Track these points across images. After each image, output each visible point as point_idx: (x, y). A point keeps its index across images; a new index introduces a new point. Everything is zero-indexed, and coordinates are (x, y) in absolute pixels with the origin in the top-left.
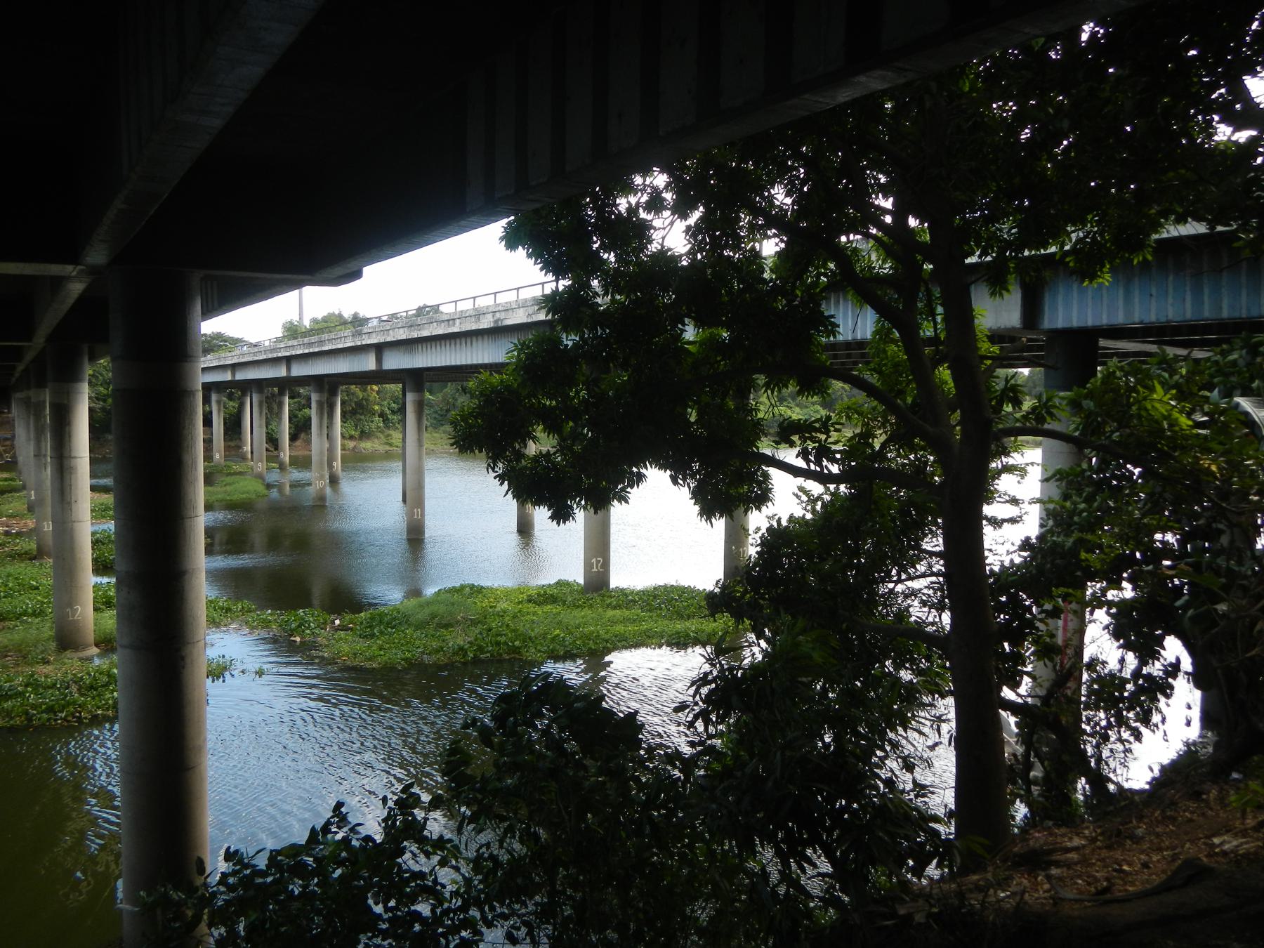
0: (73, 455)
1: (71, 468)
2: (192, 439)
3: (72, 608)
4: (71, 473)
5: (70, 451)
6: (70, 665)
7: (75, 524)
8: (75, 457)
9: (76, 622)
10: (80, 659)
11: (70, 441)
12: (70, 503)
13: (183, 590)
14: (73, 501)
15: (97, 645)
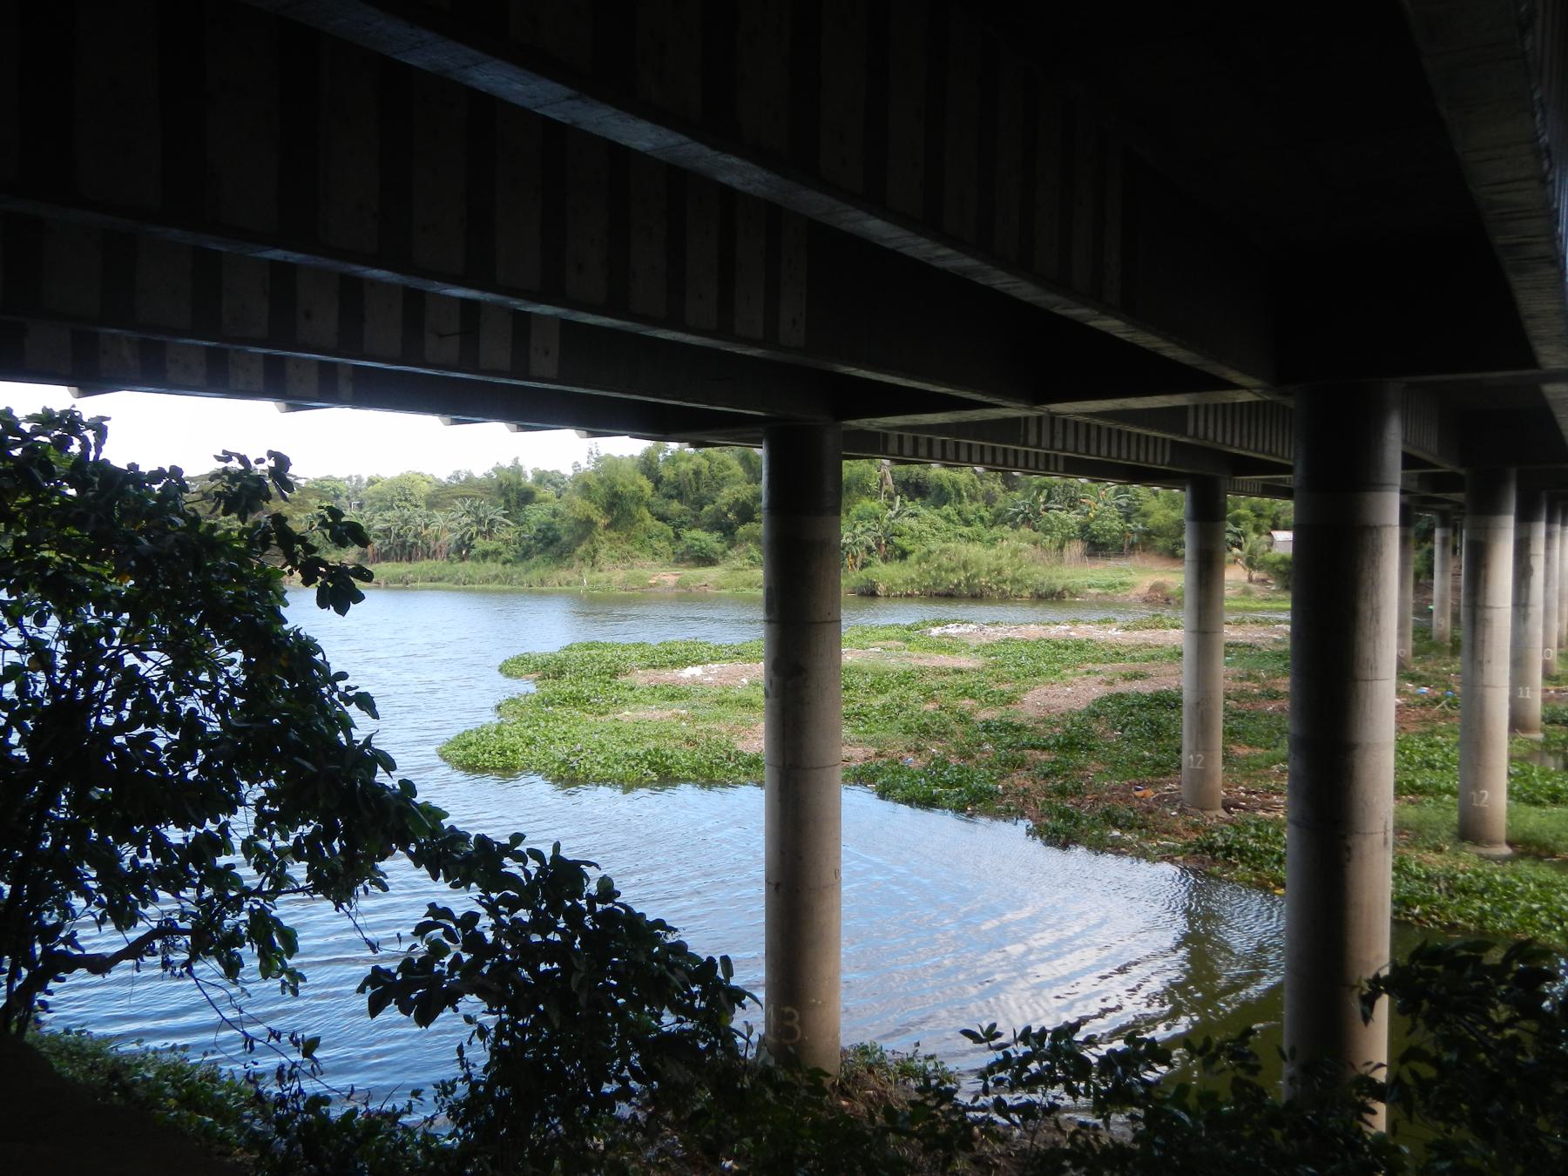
0: (1489, 603)
1: (1486, 619)
2: (1373, 584)
3: (1478, 792)
4: (1484, 626)
5: (1485, 598)
6: (1466, 862)
7: (1488, 690)
8: (1491, 608)
9: (1480, 810)
10: (1480, 856)
11: (1485, 588)
12: (1481, 663)
13: (1353, 767)
14: (1485, 660)
15: (1510, 844)
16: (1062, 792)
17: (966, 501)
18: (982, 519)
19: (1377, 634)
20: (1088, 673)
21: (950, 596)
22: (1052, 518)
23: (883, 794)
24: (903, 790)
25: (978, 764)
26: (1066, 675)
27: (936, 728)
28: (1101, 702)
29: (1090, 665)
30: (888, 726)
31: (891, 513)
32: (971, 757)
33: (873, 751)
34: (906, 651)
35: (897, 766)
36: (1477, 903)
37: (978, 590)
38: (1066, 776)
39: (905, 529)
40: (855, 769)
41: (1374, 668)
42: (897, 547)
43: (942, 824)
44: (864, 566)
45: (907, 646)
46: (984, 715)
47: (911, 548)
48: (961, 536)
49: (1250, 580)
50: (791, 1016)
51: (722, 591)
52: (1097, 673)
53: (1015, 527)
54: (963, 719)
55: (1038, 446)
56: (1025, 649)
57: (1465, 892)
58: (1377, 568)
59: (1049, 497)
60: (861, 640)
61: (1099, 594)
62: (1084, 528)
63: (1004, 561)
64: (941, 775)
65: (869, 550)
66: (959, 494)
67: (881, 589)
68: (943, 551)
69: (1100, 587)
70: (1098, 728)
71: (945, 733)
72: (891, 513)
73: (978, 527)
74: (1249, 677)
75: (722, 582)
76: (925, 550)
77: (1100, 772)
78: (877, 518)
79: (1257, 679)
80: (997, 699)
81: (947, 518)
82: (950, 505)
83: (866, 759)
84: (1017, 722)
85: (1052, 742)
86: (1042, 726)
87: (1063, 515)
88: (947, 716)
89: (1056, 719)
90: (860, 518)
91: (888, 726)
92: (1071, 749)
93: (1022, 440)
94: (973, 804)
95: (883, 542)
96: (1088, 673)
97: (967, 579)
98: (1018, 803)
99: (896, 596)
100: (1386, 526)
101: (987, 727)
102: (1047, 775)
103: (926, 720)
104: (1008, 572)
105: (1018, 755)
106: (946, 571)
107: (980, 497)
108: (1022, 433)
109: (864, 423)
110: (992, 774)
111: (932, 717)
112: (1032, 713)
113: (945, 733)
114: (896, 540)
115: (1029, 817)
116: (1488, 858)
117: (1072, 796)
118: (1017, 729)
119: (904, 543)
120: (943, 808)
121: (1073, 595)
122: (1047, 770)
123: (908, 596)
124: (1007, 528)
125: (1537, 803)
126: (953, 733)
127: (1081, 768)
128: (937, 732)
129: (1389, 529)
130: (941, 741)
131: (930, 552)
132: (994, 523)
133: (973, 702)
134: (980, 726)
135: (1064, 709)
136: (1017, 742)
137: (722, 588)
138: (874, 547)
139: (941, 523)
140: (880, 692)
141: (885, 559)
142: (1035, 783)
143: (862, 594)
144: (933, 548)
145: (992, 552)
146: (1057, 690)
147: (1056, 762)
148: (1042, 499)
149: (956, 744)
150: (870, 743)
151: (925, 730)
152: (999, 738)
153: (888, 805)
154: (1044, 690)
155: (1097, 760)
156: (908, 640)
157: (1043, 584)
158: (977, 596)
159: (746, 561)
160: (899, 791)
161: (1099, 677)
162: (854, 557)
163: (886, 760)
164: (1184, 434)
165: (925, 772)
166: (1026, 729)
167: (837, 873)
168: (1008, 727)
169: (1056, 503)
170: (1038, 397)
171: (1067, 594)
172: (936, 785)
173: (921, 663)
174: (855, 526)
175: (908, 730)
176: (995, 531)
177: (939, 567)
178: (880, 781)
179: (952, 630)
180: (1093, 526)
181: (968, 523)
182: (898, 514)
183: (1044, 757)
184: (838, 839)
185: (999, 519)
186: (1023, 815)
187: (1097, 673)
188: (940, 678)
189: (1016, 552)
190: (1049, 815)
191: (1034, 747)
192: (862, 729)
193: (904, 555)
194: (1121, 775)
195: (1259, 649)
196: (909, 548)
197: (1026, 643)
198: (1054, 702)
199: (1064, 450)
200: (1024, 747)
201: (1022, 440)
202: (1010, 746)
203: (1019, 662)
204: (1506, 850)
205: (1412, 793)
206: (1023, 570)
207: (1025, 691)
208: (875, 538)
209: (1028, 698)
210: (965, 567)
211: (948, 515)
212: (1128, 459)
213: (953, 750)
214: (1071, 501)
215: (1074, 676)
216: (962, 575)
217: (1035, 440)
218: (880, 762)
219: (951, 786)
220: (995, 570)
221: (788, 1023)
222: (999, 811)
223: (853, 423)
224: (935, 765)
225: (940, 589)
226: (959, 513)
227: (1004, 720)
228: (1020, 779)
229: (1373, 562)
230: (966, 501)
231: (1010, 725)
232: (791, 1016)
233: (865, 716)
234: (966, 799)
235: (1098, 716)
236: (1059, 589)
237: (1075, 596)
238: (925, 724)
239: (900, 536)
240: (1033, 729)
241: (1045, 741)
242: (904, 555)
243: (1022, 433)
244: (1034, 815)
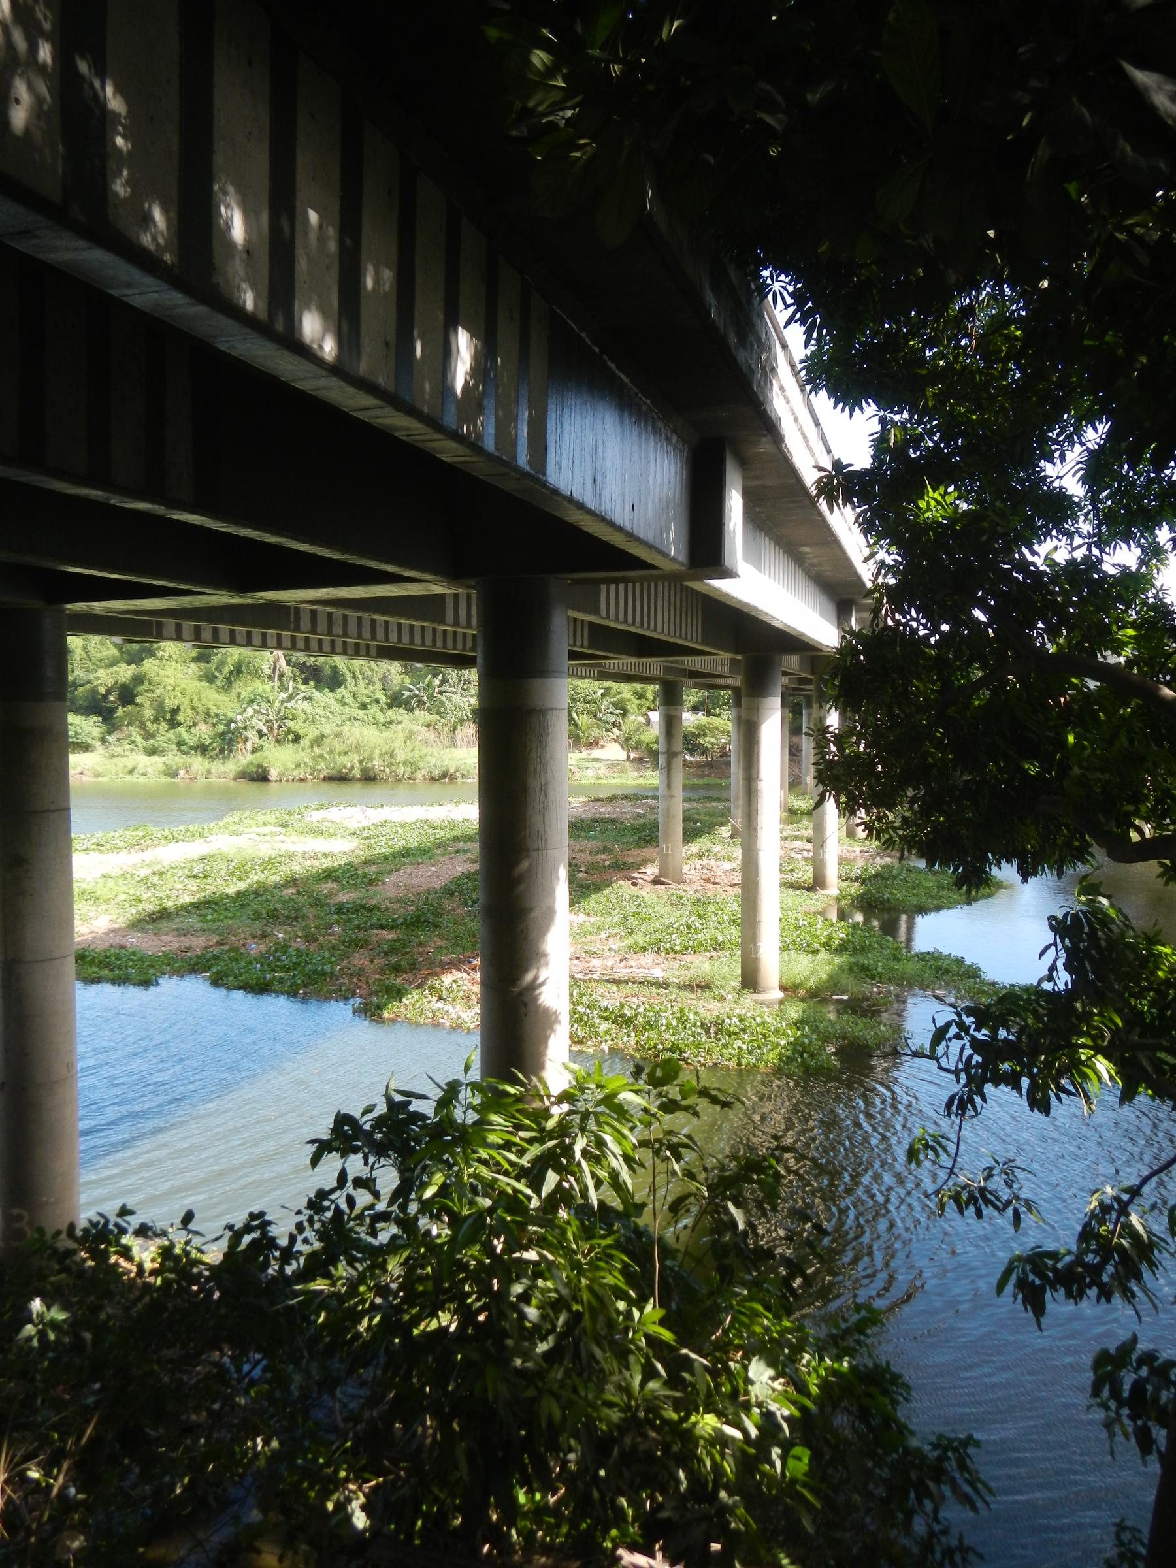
10: (756, 1001)
12: (756, 830)
15: (782, 988)
16: (397, 969)
17: (362, 683)
18: (377, 701)
19: (546, 807)
20: (457, 852)
21: (340, 778)
22: (447, 702)
23: (216, 983)
24: (236, 977)
25: (321, 946)
26: (436, 854)
27: (286, 913)
28: (457, 881)
29: (461, 844)
30: (238, 914)
31: (284, 696)
32: (316, 940)
33: (214, 939)
34: (281, 837)
35: (237, 954)
36: (739, 1043)
37: (371, 774)
38: (407, 953)
39: (298, 713)
40: (191, 959)
41: (543, 839)
42: (289, 731)
43: (278, 1006)
44: (253, 752)
45: (283, 830)
46: (343, 897)
47: (304, 731)
48: (356, 719)
49: (628, 757)
50: (20, 1218)
51: (100, 779)
52: (465, 852)
53: (411, 710)
54: (318, 903)
55: (313, 631)
56: (400, 831)
57: (730, 1034)
58: (544, 748)
60: (235, 827)
64: (279, 960)
65: (261, 734)
66: (354, 677)
67: (273, 774)
68: (338, 735)
70: (448, 905)
71: (296, 918)
72: (284, 696)
73: (374, 709)
74: (605, 850)
75: (100, 769)
76: (318, 733)
77: (441, 947)
78: (269, 701)
79: (611, 852)
80: (359, 881)
81: (342, 702)
82: (346, 688)
83: (206, 948)
84: (373, 902)
85: (400, 921)
86: (394, 906)
87: (455, 698)
88: (302, 900)
89: (413, 898)
90: (251, 701)
91: (238, 914)
92: (418, 927)
93: (292, 626)
94: (305, 986)
95: (275, 726)
96: (457, 852)
97: (360, 762)
98: (351, 983)
99: (288, 781)
100: (552, 709)
101: (340, 908)
102: (386, 954)
103: (278, 906)
104: (401, 756)
105: (361, 934)
106: (340, 754)
107: (376, 679)
108: (292, 618)
109: (81, 606)
110: (333, 955)
111: (285, 902)
112: (391, 893)
113: (296, 918)
114: (289, 723)
115: (361, 997)
116: (762, 1003)
117: (406, 973)
118: (370, 910)
120: (275, 991)
121: (463, 775)
122: (386, 948)
123: (301, 780)
124: (402, 710)
125: (815, 952)
126: (305, 917)
127: (420, 945)
128: (288, 917)
129: (554, 712)
130: (290, 925)
131: (323, 735)
132: (390, 706)
133: (335, 885)
134: (333, 909)
135: (424, 887)
136: (365, 922)
137: (99, 775)
138: (265, 730)
140: (240, 879)
141: (278, 741)
142: (372, 961)
143: (253, 780)
144: (326, 732)
145: (387, 734)
146: (423, 869)
147: (399, 940)
148: (437, 682)
149: (304, 929)
150: (214, 932)
151: (274, 916)
152: (350, 920)
153: (222, 992)
154: (409, 871)
155: (440, 936)
156: (284, 825)
158: (369, 778)
159: (128, 747)
160: (231, 979)
161: (466, 856)
162: (246, 739)
163: (226, 948)
164: (442, 621)
165: (262, 958)
166: (379, 909)
167: (70, 1066)
168: (361, 908)
170: (242, 588)
171: (458, 775)
172: (273, 970)
173: (292, 848)
174: (245, 710)
175: (257, 916)
176: (391, 714)
177: (331, 752)
178: (215, 970)
179: (335, 814)
181: (364, 706)
182: (290, 698)
183: (389, 936)
184: (70, 1033)
185: (396, 700)
186: (354, 995)
187: (465, 852)
188: (309, 863)
189: (411, 735)
190: (376, 993)
191: (382, 927)
192: (209, 917)
193: (297, 739)
194: (459, 949)
195: (622, 823)
196: (301, 732)
197: (402, 825)
198: (415, 881)
199: (345, 635)
200: (373, 927)
201: (292, 626)
202: (358, 927)
203: (391, 843)
204: (780, 995)
205: (715, 949)
206: (416, 753)
207: (390, 872)
208: (267, 721)
209: (391, 879)
210: (358, 751)
212: (423, 644)
213: (300, 934)
215: (443, 855)
216: (356, 758)
217: (325, 627)
218: (216, 951)
219: (288, 970)
220: (386, 753)
221: (17, 1225)
222: (330, 992)
223: (69, 606)
224: (276, 951)
225: (334, 772)
226: (354, 696)
227: (359, 902)
228: (359, 959)
229: (541, 742)
230: (362, 683)
231: (363, 906)
232: (20, 1218)
233: (216, 904)
234: (299, 982)
235: (452, 894)
236: (452, 771)
237: (467, 778)
238: (276, 910)
240: (387, 909)
241: (394, 920)
242: (297, 739)
243: (292, 618)
244: (364, 992)
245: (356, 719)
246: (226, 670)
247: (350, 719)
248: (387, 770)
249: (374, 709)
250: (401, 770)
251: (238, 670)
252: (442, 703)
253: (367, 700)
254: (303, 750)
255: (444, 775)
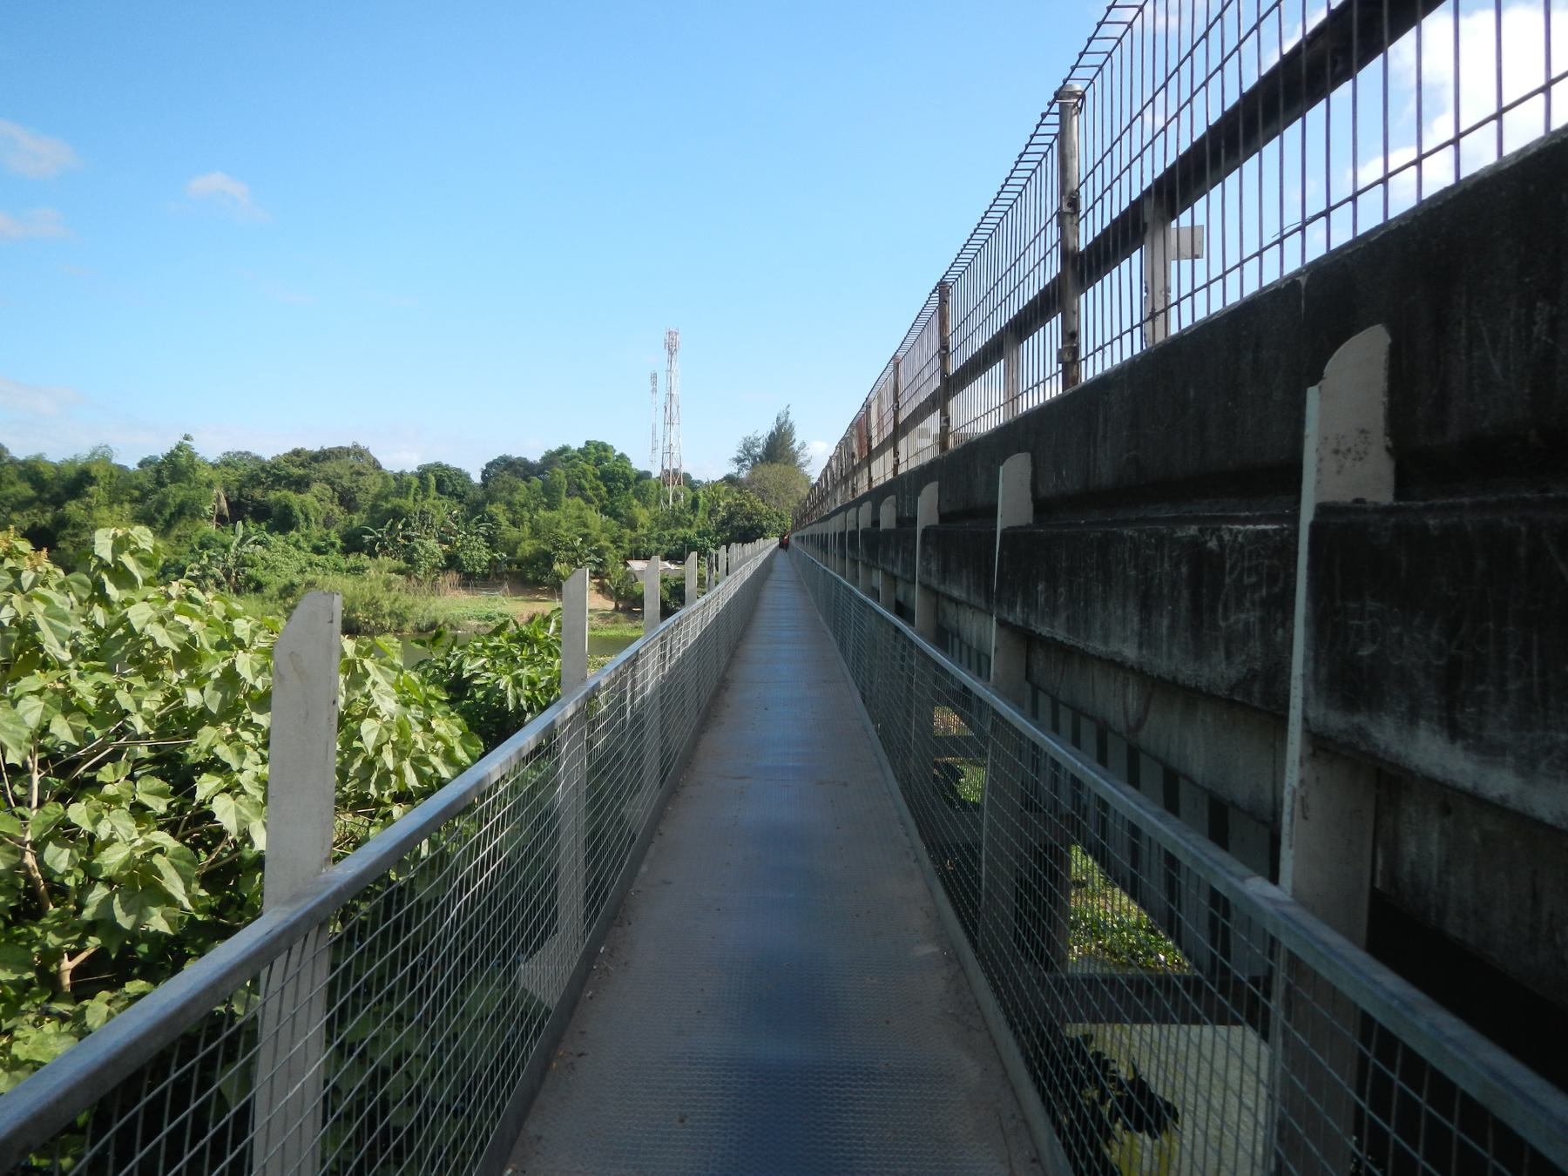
17: (313, 525)
18: (333, 545)
37: (354, 626)
42: (249, 579)
48: (317, 565)
53: (373, 554)
59: (406, 525)
61: (479, 626)
62: (452, 562)
63: (378, 595)
66: (307, 519)
69: (479, 619)
76: (286, 581)
81: (297, 545)
82: (298, 531)
104: (386, 606)
114: (249, 571)
119: (258, 573)
121: (452, 627)
124: (363, 556)
132: (346, 551)
139: (291, 547)
144: (297, 580)
157: (423, 617)
169: (413, 531)
174: (201, 558)
176: (352, 559)
180: (461, 555)
181: (317, 550)
185: (353, 543)
189: (388, 585)
211: (298, 541)
214: (428, 527)
230: (313, 525)
236: (441, 622)
239: (252, 567)
245: (317, 565)
246: (167, 513)
247: (310, 564)
248: (373, 623)
249: (334, 556)
250: (387, 622)
251: (180, 512)
252: (415, 550)
253: (323, 543)
254: (271, 599)
255: (433, 625)
